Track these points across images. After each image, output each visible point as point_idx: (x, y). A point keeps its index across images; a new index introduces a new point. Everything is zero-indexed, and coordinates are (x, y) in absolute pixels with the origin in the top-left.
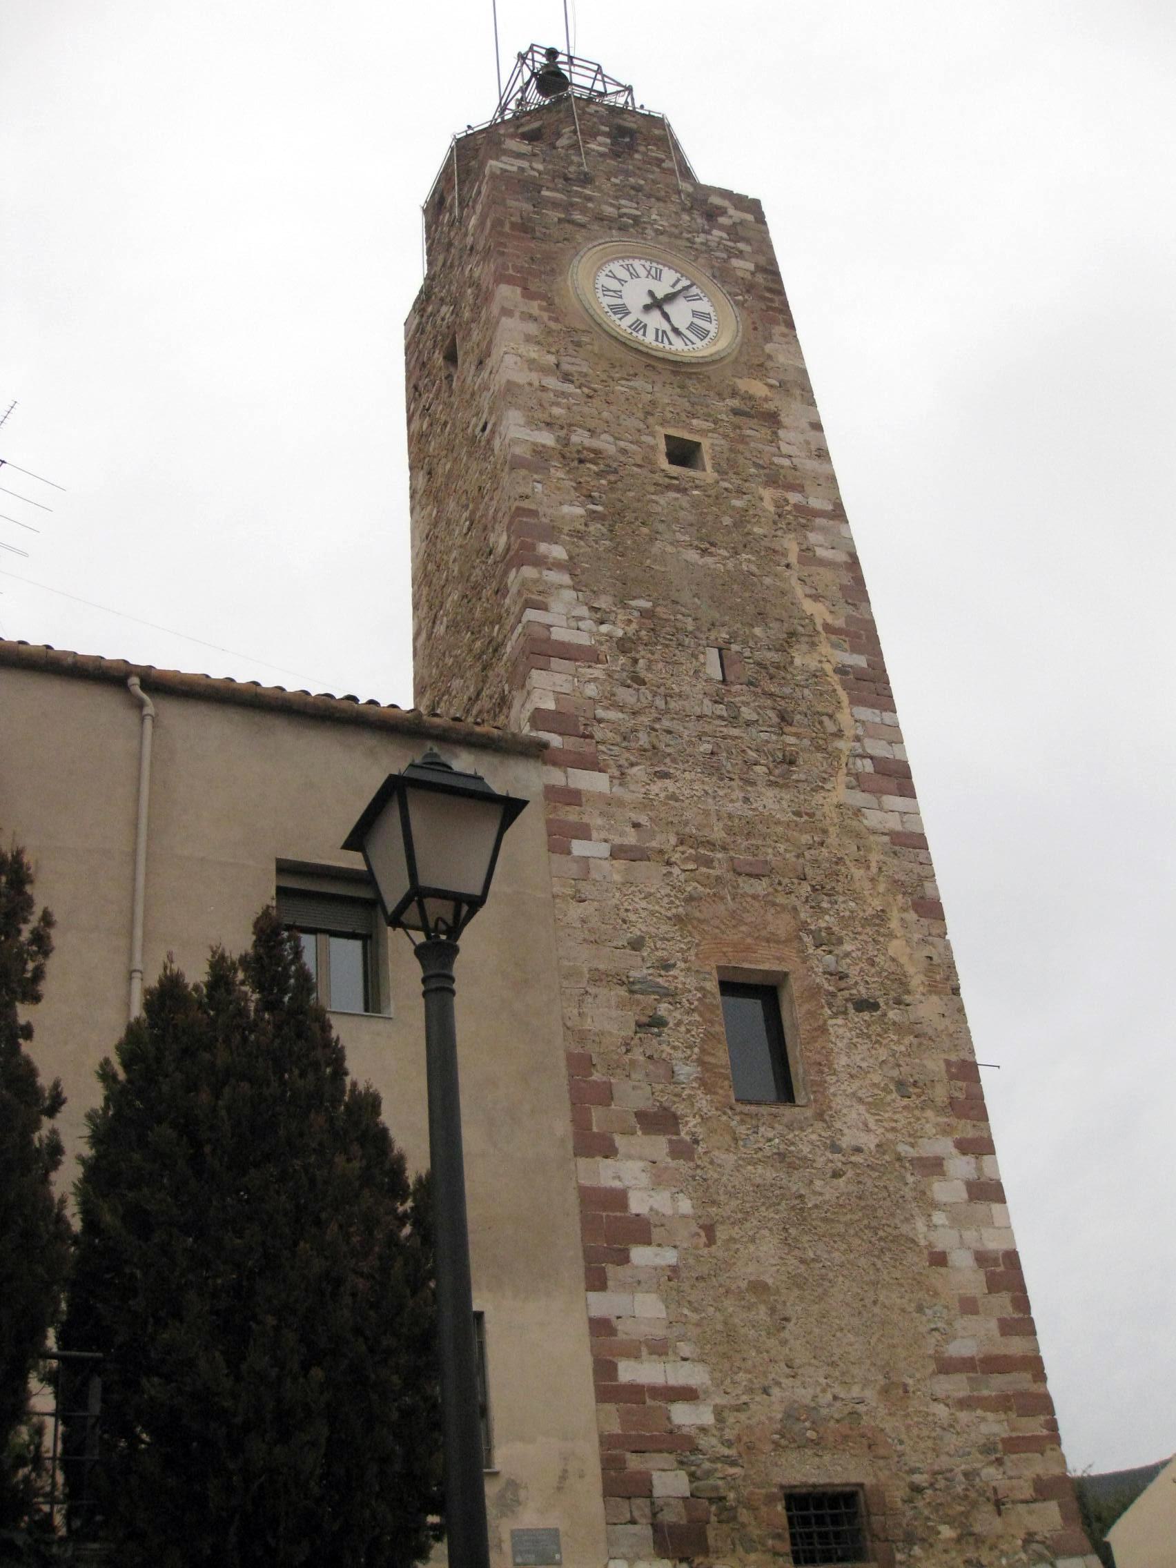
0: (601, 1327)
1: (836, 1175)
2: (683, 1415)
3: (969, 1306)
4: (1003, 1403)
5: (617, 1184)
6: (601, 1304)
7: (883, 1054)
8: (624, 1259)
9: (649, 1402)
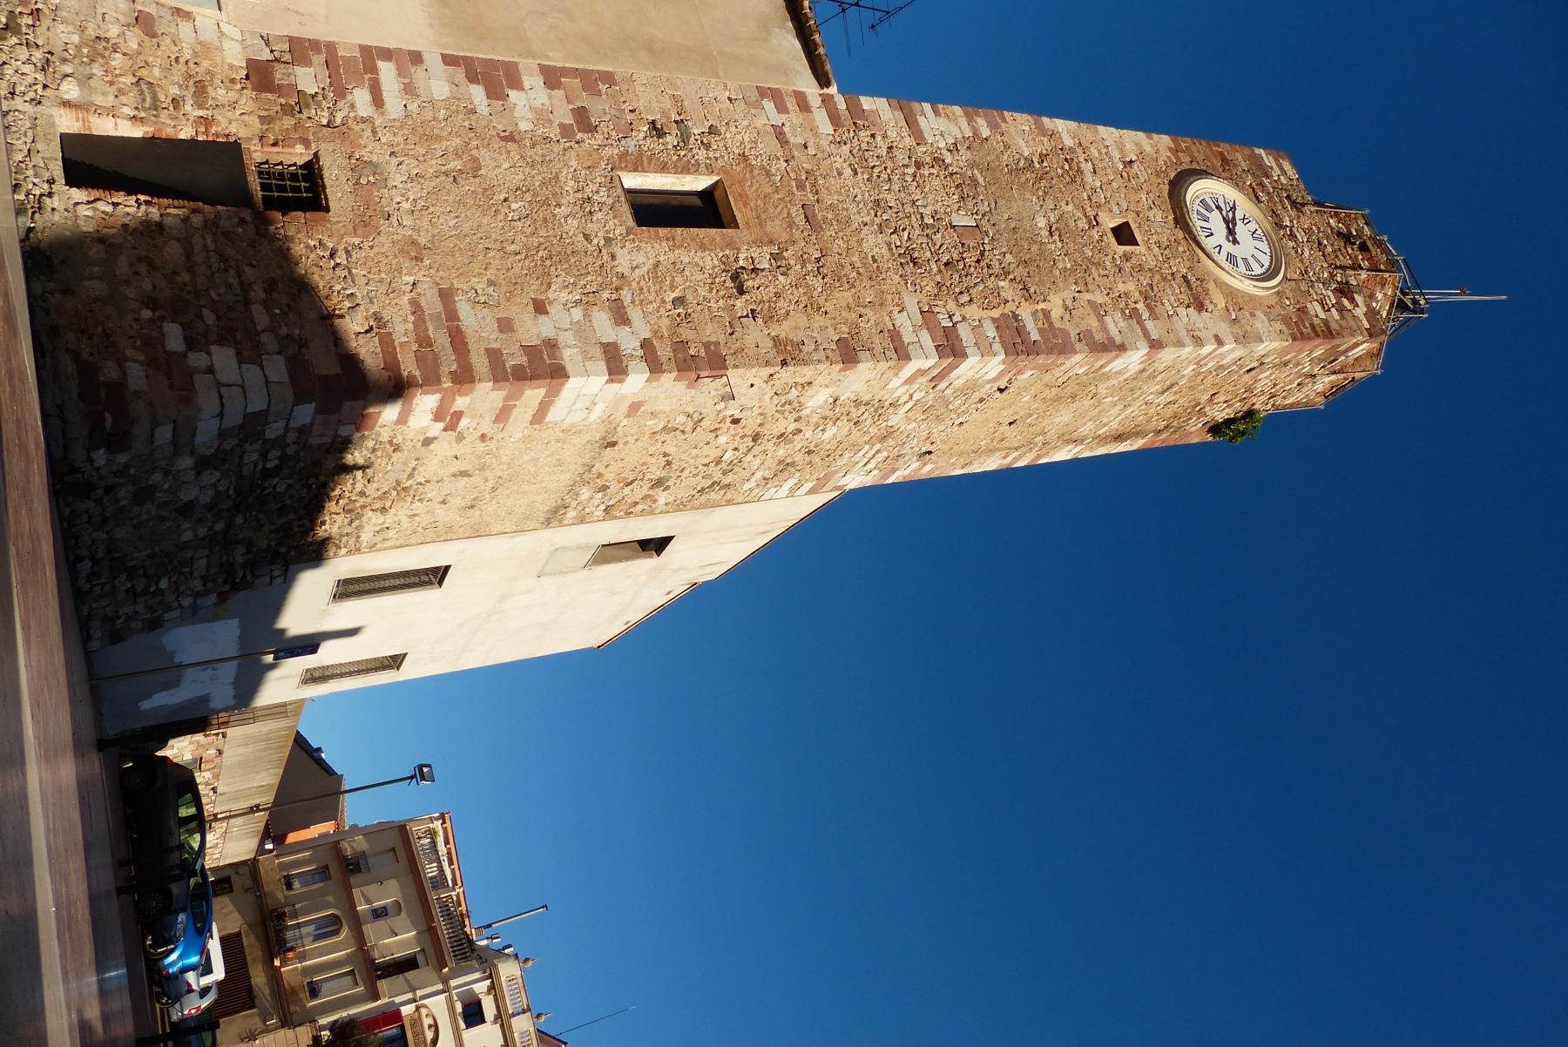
0: (416, 58)
1: (587, 237)
2: (361, 97)
3: (505, 325)
4: (424, 341)
5: (527, 85)
6: (433, 60)
7: (703, 292)
8: (472, 78)
9: (367, 77)
